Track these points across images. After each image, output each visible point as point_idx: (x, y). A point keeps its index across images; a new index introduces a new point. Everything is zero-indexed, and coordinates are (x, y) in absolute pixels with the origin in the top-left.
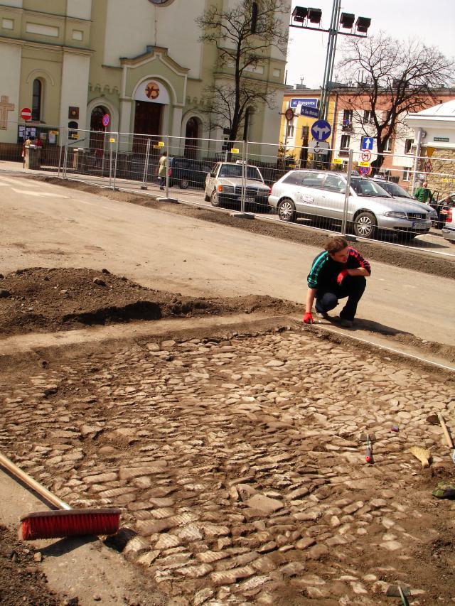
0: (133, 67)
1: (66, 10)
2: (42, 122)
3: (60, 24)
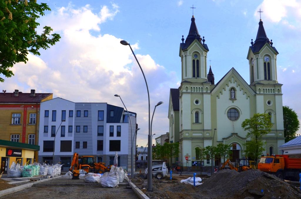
3: (202, 132)
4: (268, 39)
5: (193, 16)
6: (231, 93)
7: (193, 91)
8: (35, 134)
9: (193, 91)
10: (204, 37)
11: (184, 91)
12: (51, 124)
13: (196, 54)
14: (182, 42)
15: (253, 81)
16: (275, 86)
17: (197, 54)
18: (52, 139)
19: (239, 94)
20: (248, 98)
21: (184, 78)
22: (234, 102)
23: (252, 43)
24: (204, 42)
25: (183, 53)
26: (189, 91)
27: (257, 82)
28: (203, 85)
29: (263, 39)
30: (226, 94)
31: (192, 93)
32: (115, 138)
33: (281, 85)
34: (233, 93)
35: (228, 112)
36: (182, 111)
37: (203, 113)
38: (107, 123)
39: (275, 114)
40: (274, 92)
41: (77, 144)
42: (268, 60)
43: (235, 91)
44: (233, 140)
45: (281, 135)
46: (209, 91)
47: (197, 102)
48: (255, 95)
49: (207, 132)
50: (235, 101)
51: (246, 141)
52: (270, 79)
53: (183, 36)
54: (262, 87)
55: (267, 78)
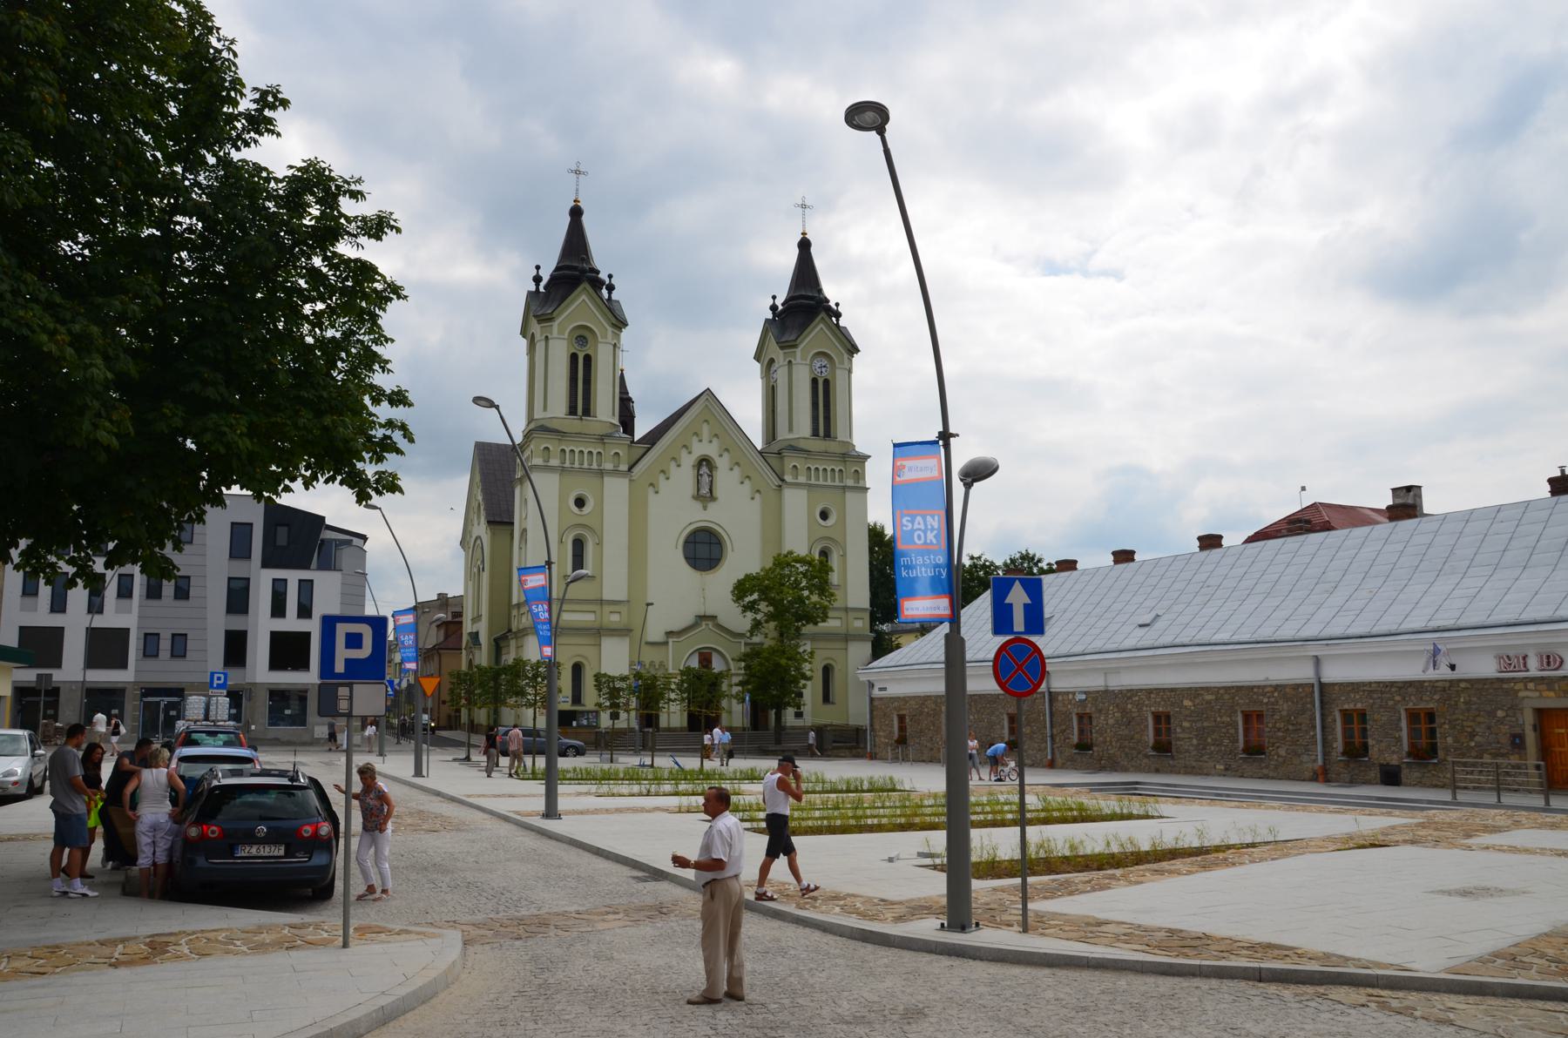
0: (680, 640)
1: (602, 597)
2: (584, 705)
4: (828, 301)
5: (575, 201)
6: (699, 475)
7: (567, 464)
9: (567, 464)
10: (610, 276)
11: (538, 461)
13: (582, 336)
14: (533, 288)
15: (774, 439)
16: (845, 461)
17: (587, 334)
19: (726, 479)
20: (757, 495)
21: (536, 417)
22: (709, 509)
23: (773, 308)
24: (610, 293)
25: (535, 328)
26: (554, 462)
27: (787, 443)
28: (604, 443)
29: (812, 298)
30: (683, 477)
31: (562, 470)
33: (864, 458)
34: (706, 475)
35: (687, 542)
36: (524, 532)
37: (600, 544)
38: (262, 570)
39: (844, 556)
40: (841, 480)
41: (151, 643)
42: (824, 369)
43: (711, 472)
44: (705, 638)
45: (858, 624)
46: (624, 467)
47: (580, 502)
48: (780, 486)
49: (612, 608)
50: (711, 506)
51: (746, 644)
52: (828, 435)
53: (538, 268)
54: (803, 459)
55: (821, 432)
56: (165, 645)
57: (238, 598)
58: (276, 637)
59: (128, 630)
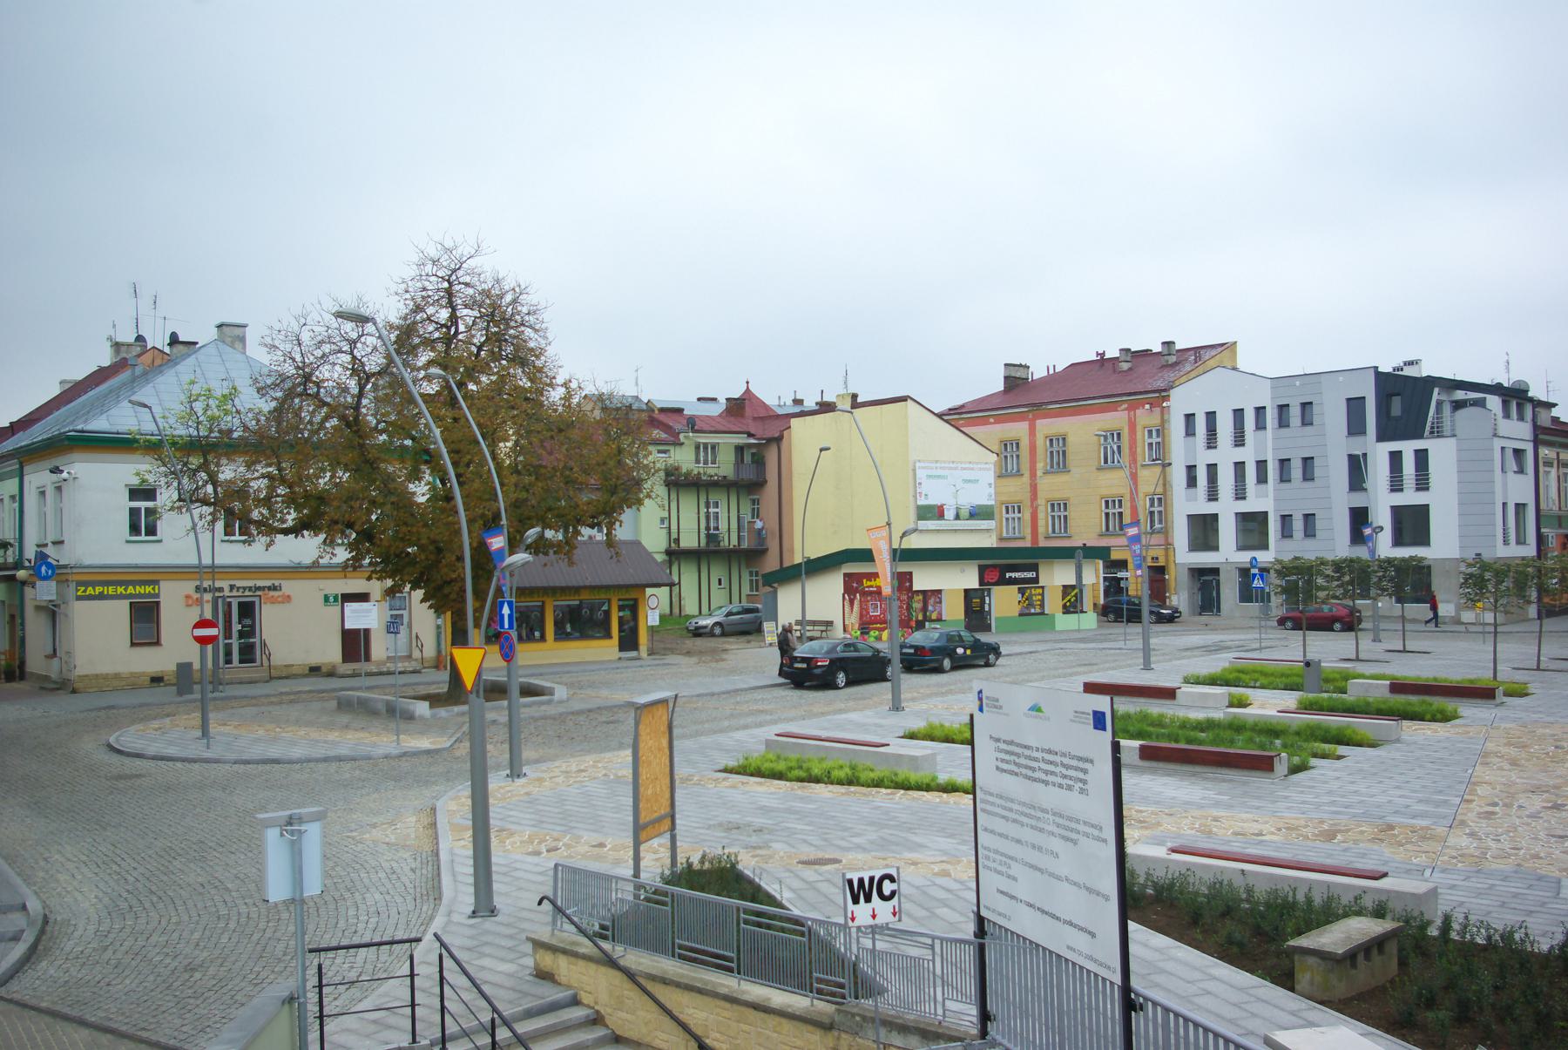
8: (1165, 493)
12: (1203, 458)
18: (1208, 508)
32: (1410, 497)
56: (1298, 525)
57: (1357, 468)
58: (1397, 511)
59: (1267, 512)
